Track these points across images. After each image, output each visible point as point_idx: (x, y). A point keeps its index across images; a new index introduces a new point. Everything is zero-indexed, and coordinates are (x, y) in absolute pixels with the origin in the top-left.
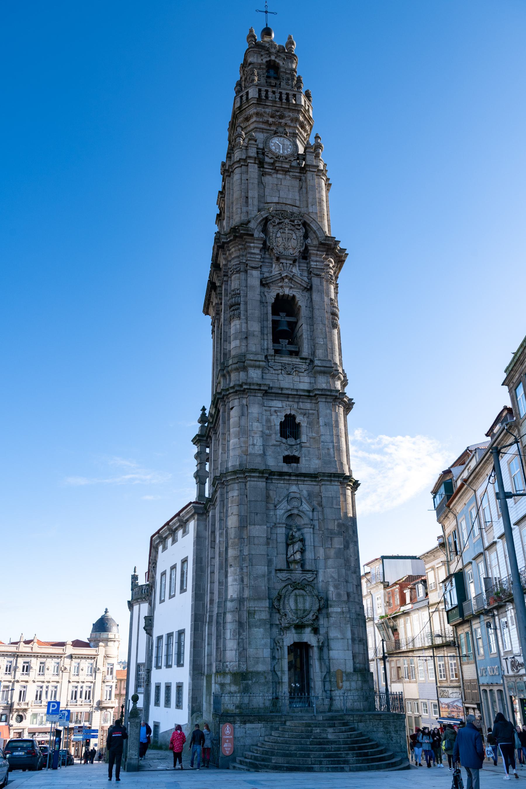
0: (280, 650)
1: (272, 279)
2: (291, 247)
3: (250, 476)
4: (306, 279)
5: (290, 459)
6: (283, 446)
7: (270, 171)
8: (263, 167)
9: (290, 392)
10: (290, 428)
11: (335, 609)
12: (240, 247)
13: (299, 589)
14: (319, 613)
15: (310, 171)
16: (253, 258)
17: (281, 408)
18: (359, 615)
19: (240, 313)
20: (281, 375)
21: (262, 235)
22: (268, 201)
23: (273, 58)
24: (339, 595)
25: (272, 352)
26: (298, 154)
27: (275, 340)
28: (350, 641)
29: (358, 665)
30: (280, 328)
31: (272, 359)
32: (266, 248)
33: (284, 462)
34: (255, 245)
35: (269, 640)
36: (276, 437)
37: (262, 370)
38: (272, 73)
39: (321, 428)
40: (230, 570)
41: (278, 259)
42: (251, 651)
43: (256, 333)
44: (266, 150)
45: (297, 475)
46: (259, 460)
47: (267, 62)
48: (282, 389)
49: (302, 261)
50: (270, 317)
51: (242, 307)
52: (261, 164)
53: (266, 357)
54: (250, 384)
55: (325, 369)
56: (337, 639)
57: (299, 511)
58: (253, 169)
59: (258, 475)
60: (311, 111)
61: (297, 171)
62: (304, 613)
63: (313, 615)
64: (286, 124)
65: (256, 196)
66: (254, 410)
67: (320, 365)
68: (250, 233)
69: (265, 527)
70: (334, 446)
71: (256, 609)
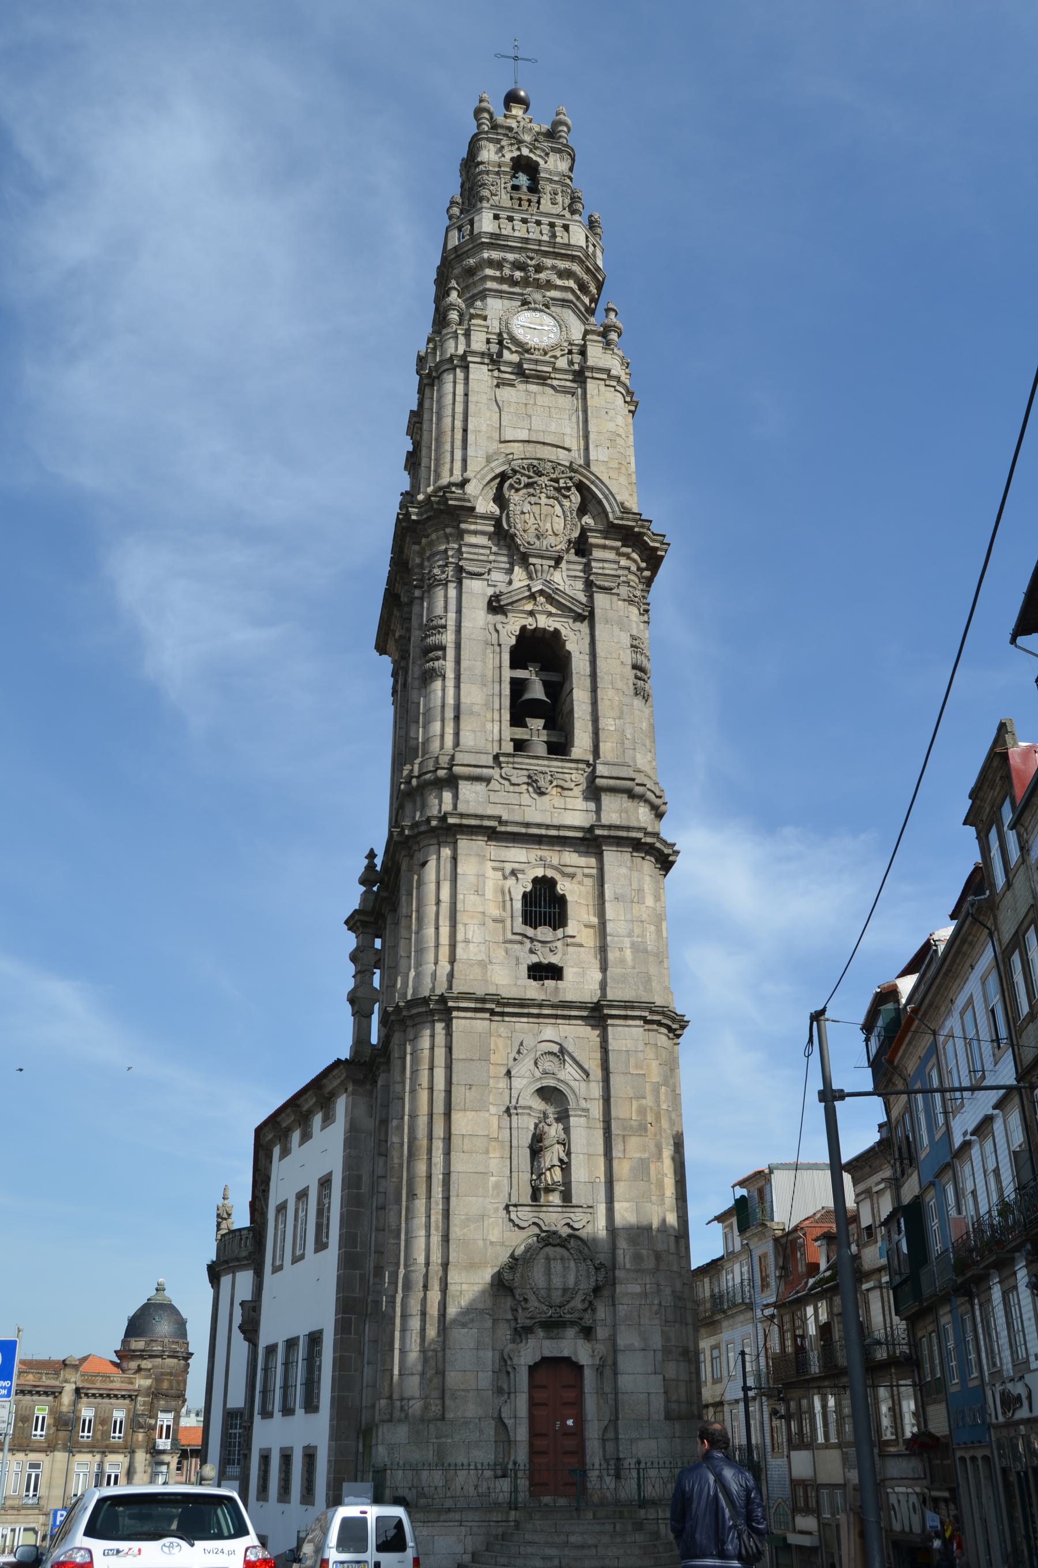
0: (512, 1375)
1: (511, 597)
2: (550, 532)
3: (459, 1009)
5: (545, 971)
6: (528, 944)
7: (513, 377)
8: (499, 370)
9: (543, 832)
10: (544, 906)
11: (629, 1288)
12: (448, 530)
13: (554, 1246)
14: (595, 1297)
15: (593, 378)
16: (474, 554)
18: (680, 1299)
20: (526, 795)
22: (507, 439)
23: (525, 152)
24: (637, 1257)
25: (509, 747)
26: (570, 344)
27: (517, 720)
28: (659, 1355)
29: (674, 1406)
30: (528, 696)
31: (508, 763)
33: (529, 977)
34: (479, 528)
35: (490, 1354)
38: (523, 180)
39: (607, 905)
41: (524, 560)
42: (453, 1378)
43: (476, 708)
44: (505, 336)
45: (553, 1006)
46: (476, 972)
47: (512, 159)
48: (527, 825)
51: (450, 653)
52: (494, 361)
53: (496, 757)
54: (462, 816)
55: (618, 782)
56: (630, 1349)
57: (559, 1080)
58: (480, 374)
59: (472, 1005)
60: (599, 253)
61: (566, 377)
62: (563, 1296)
63: (583, 1300)
64: (548, 281)
65: (484, 428)
67: (606, 774)
68: (469, 504)
69: (487, 1115)
70: (633, 944)
71: (465, 1287)
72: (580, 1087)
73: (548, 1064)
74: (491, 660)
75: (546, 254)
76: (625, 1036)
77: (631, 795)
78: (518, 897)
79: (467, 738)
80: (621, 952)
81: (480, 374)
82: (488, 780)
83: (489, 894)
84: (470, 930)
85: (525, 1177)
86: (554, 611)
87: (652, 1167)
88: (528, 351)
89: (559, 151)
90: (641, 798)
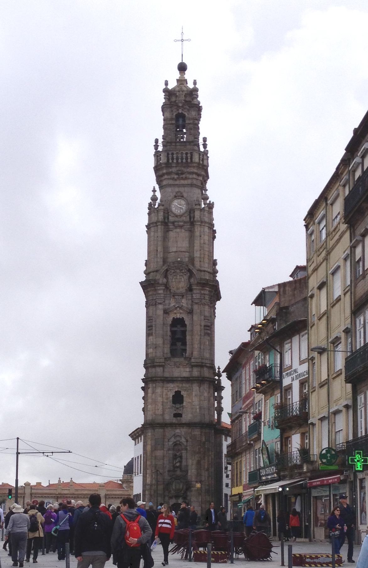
4: (190, 306)
10: (178, 398)
17: (173, 388)
19: (152, 333)
21: (165, 280)
23: (180, 111)
25: (169, 355)
27: (173, 344)
33: (174, 417)
36: (170, 404)
37: (164, 368)
40: (148, 471)
41: (174, 296)
46: (160, 417)
47: (176, 115)
48: (172, 378)
49: (190, 293)
50: (169, 333)
51: (154, 328)
66: (159, 390)
72: (185, 443)
75: (184, 167)
76: (197, 432)
82: (163, 366)
83: (164, 396)
86: (182, 312)
88: (177, 216)
89: (193, 107)
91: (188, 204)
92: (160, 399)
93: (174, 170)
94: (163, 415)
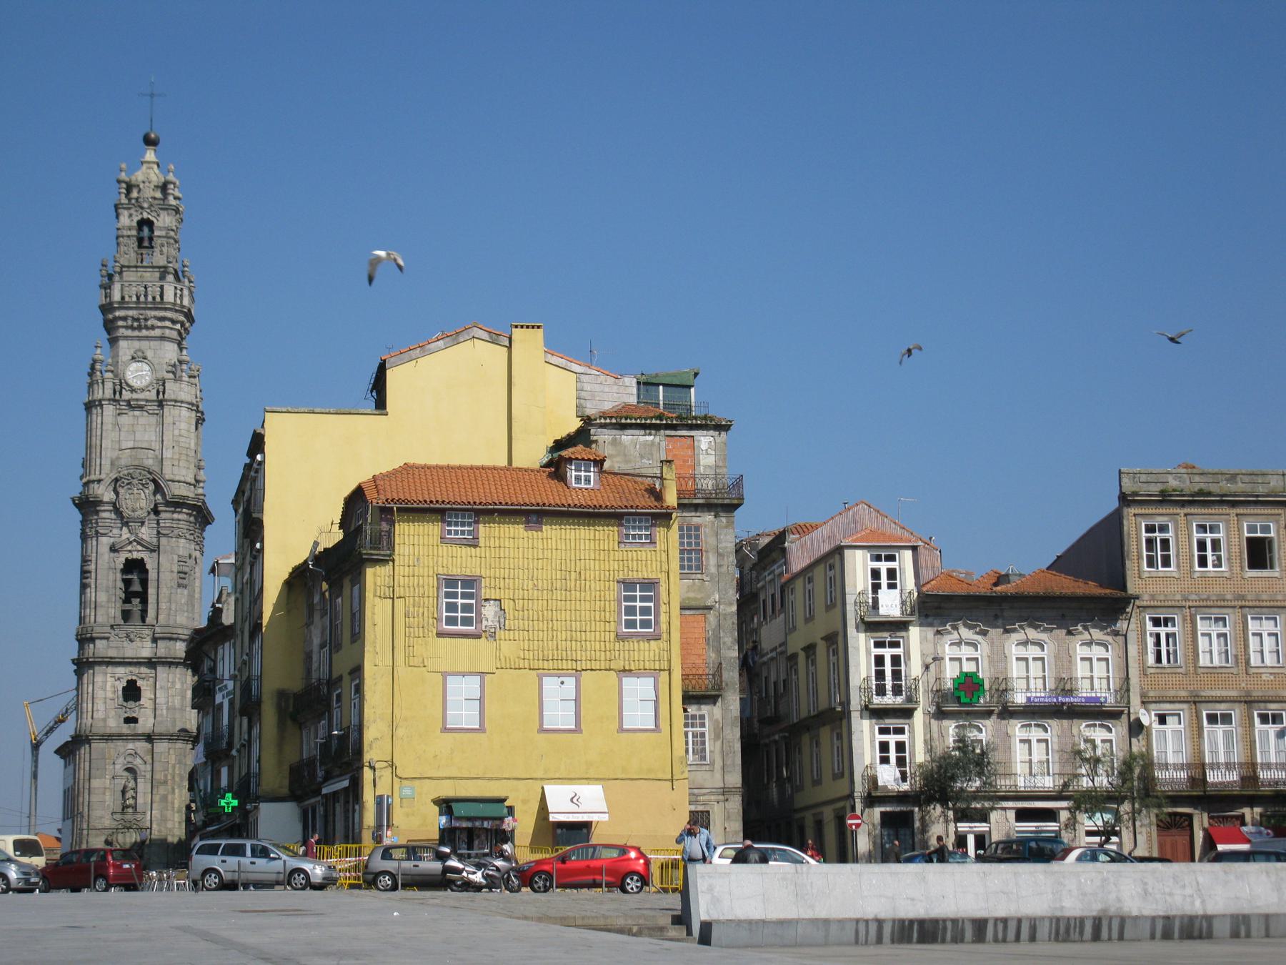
5: (131, 720)
10: (132, 692)
23: (145, 215)
27: (127, 600)
32: (117, 511)
41: (126, 524)
46: (101, 724)
51: (93, 575)
58: (109, 410)
72: (142, 767)
73: (129, 759)
74: (111, 577)
75: (150, 309)
76: (161, 746)
77: (170, 639)
78: (120, 689)
79: (99, 619)
80: (162, 711)
81: (109, 410)
82: (107, 638)
83: (108, 688)
84: (100, 706)
85: (120, 801)
86: (140, 548)
87: (170, 797)
90: (176, 639)
91: (153, 370)
92: (100, 694)
93: (130, 313)
94: (105, 720)
